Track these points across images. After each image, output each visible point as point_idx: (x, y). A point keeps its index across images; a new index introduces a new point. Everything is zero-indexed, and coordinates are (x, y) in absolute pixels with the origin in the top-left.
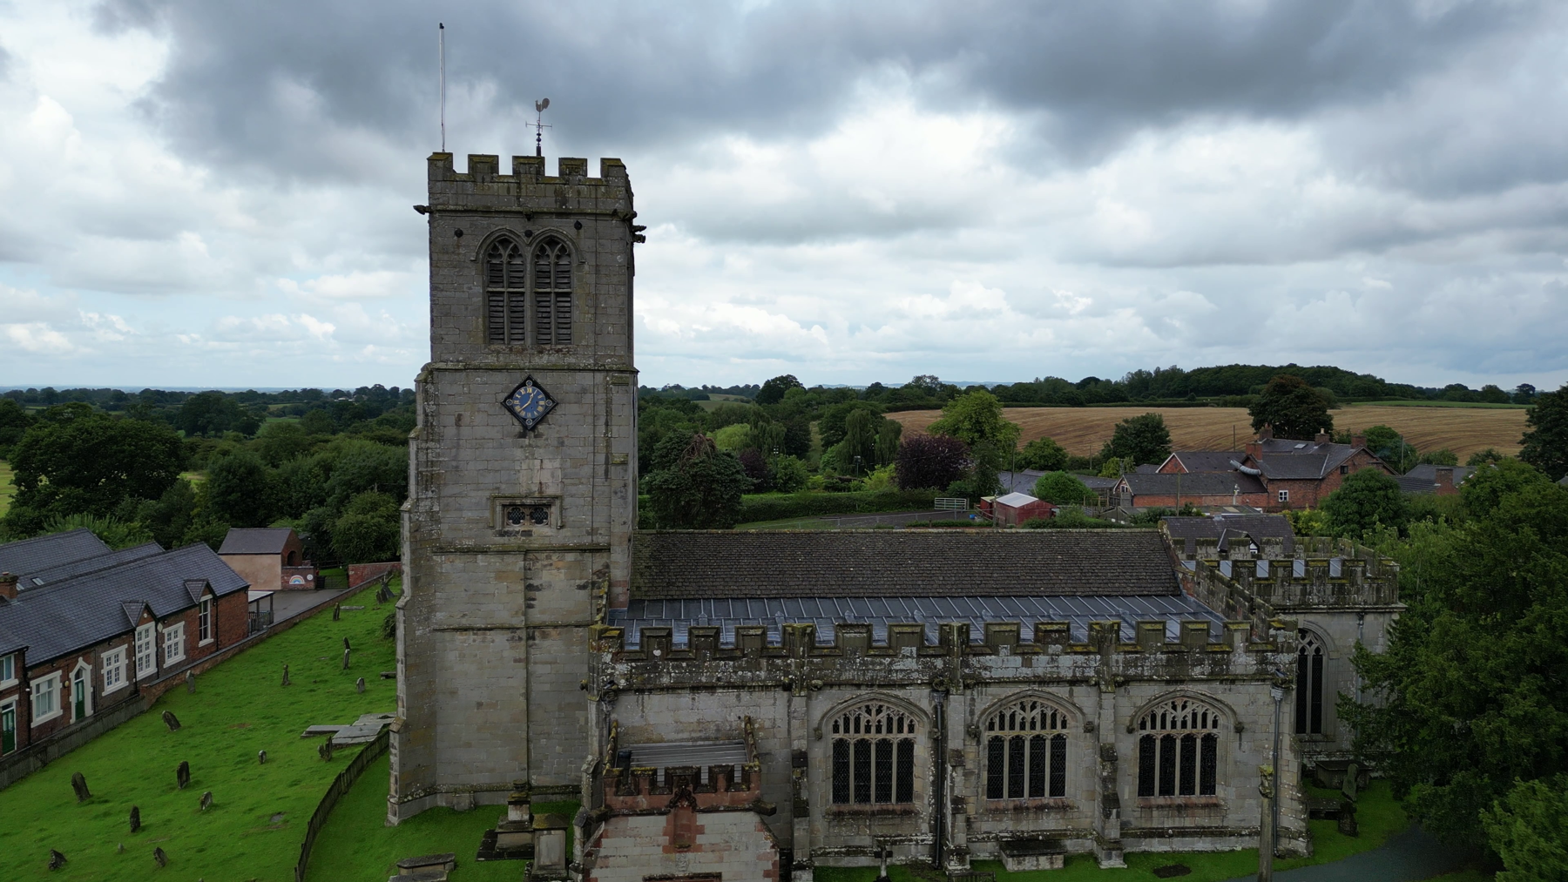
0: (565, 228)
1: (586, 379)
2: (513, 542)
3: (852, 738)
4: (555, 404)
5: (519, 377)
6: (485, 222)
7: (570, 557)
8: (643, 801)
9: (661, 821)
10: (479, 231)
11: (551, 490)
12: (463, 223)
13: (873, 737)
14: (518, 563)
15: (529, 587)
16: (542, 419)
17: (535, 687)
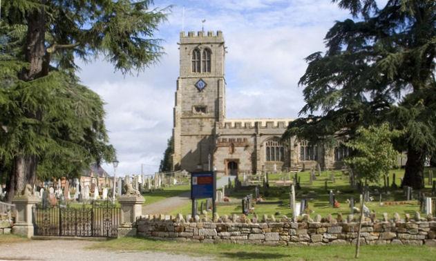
0: (209, 46)
1: (213, 79)
2: (198, 116)
3: (270, 146)
4: (206, 85)
5: (198, 79)
6: (191, 46)
7: (210, 119)
8: (225, 144)
9: (228, 148)
10: (191, 49)
11: (206, 104)
12: (187, 46)
13: (275, 146)
14: (198, 120)
15: (201, 126)
16: (203, 88)
17: (202, 149)
